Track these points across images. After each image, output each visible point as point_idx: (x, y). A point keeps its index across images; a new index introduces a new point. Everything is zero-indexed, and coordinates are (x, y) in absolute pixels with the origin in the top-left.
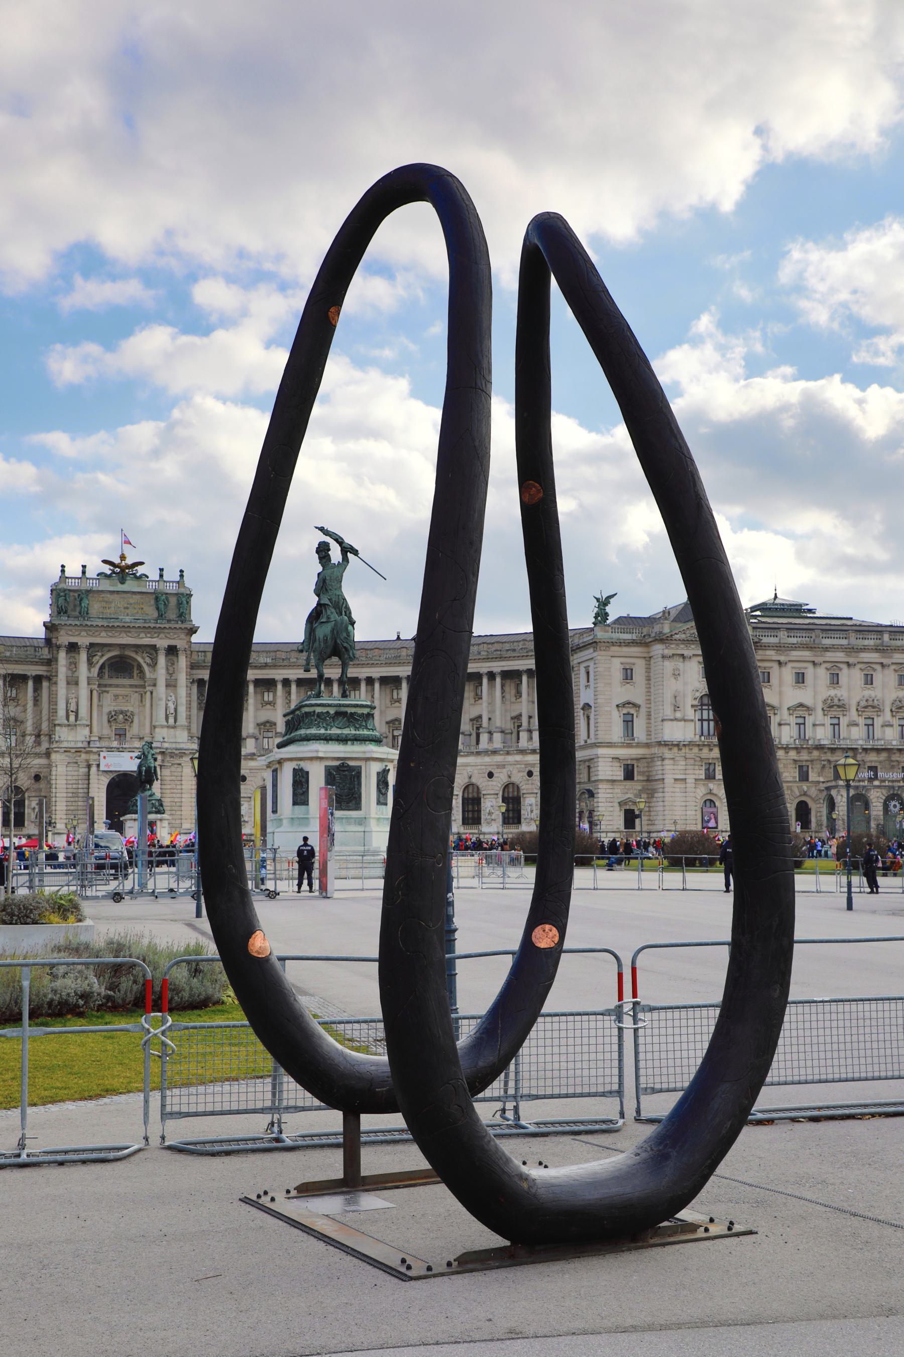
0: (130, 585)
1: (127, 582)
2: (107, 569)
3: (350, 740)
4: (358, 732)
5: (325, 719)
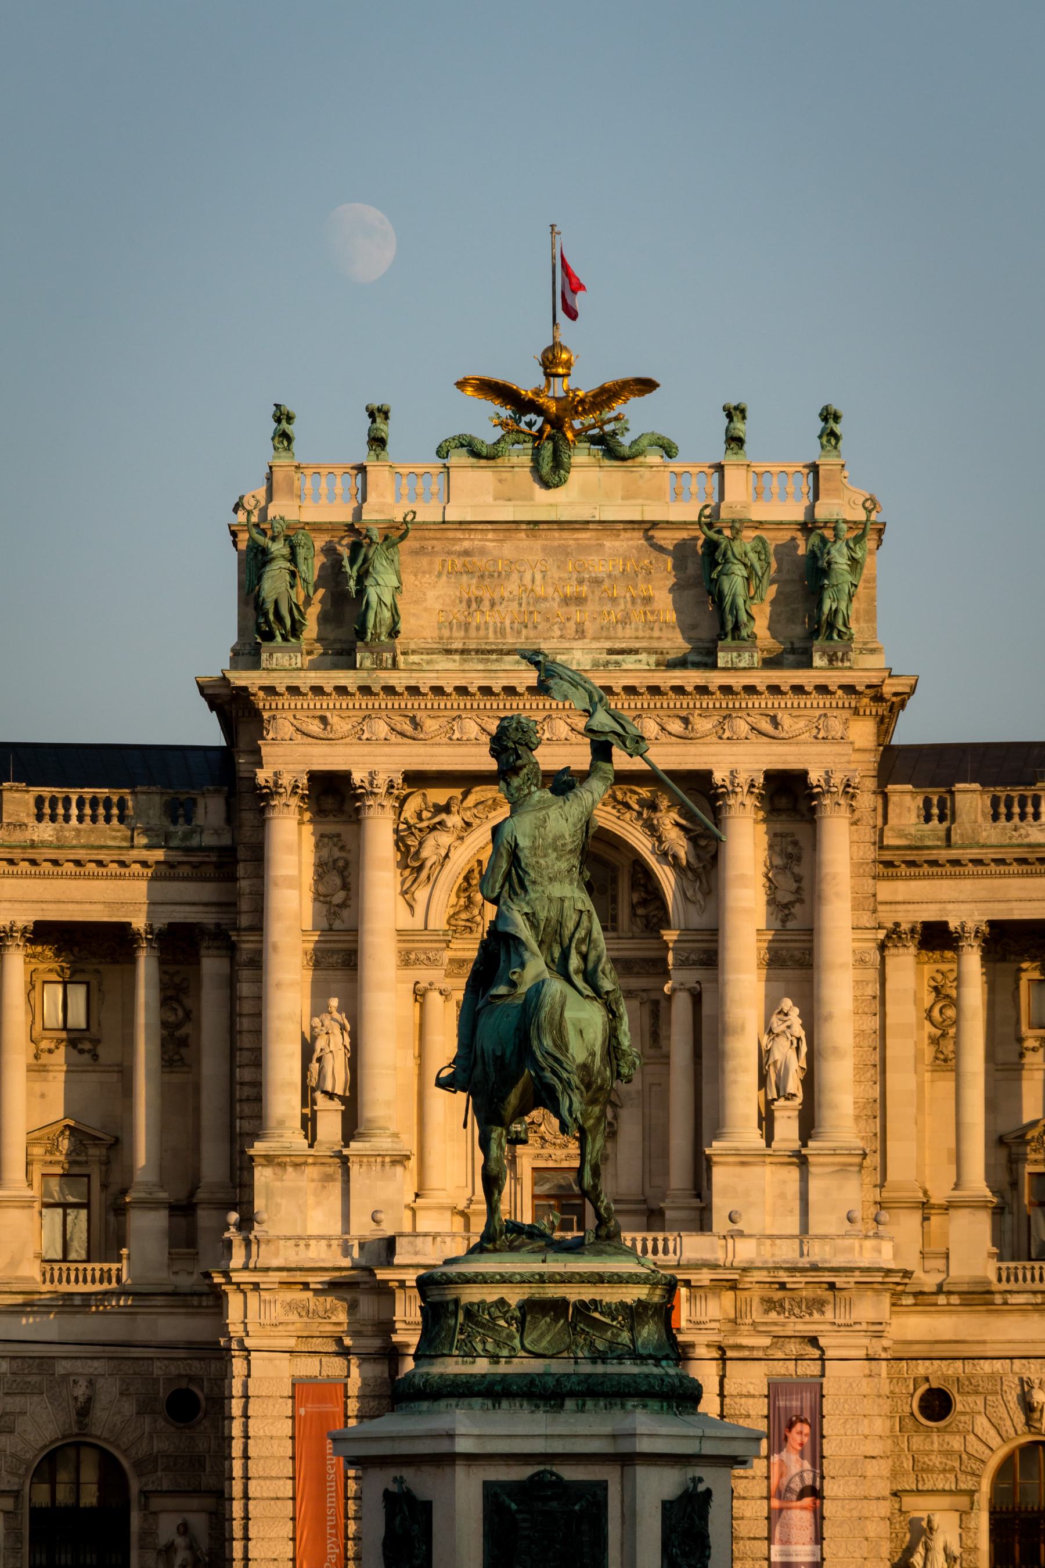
0: (589, 487)
1: (575, 477)
2: (484, 419)
3: (572, 1394)
4: (600, 1369)
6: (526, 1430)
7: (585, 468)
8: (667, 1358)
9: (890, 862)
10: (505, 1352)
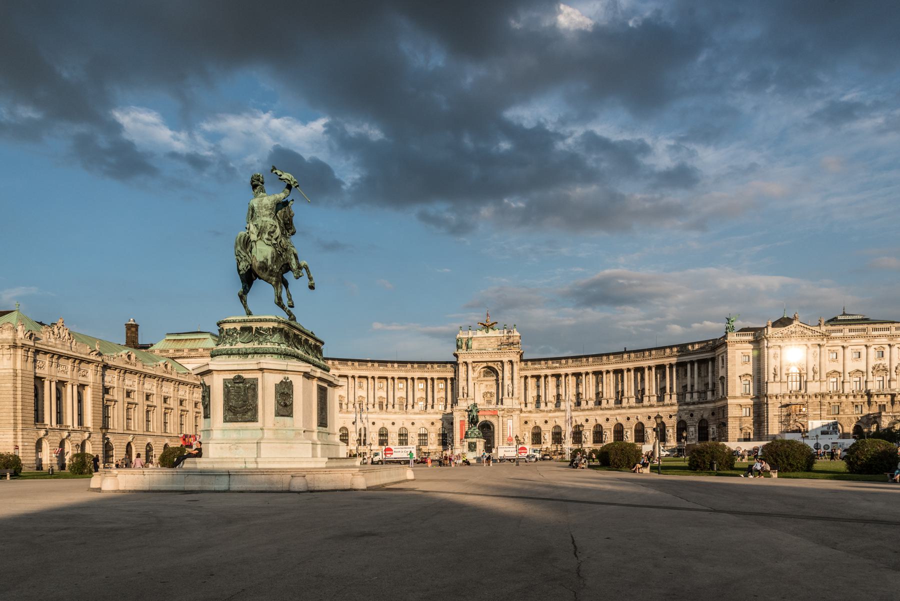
0: (491, 333)
5: (232, 336)
6: (236, 363)
7: (490, 330)
9: (521, 370)
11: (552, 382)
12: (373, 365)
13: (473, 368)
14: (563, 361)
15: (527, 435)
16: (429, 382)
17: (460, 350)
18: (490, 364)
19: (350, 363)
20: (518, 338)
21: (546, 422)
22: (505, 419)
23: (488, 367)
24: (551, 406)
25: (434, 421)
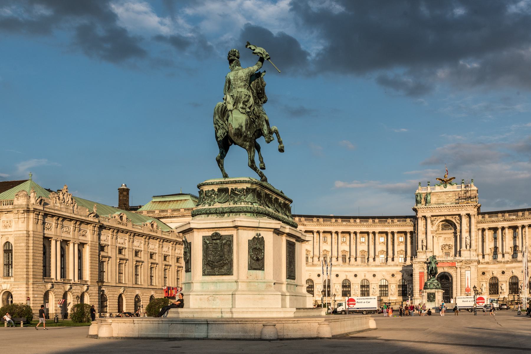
3: (226, 212)
4: (235, 206)
5: (210, 197)
8: (256, 202)
9: (478, 222)
10: (213, 203)
11: (509, 234)
12: (336, 221)
13: (432, 221)
14: (520, 214)
15: (485, 285)
16: (390, 236)
17: (419, 205)
18: (448, 218)
19: (315, 219)
20: (475, 192)
21: (503, 273)
22: (463, 271)
23: (446, 221)
24: (508, 257)
25: (394, 272)
